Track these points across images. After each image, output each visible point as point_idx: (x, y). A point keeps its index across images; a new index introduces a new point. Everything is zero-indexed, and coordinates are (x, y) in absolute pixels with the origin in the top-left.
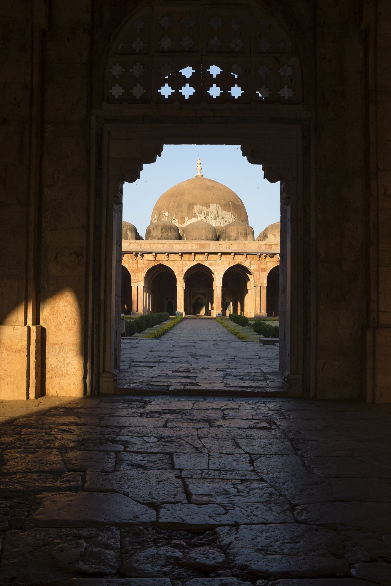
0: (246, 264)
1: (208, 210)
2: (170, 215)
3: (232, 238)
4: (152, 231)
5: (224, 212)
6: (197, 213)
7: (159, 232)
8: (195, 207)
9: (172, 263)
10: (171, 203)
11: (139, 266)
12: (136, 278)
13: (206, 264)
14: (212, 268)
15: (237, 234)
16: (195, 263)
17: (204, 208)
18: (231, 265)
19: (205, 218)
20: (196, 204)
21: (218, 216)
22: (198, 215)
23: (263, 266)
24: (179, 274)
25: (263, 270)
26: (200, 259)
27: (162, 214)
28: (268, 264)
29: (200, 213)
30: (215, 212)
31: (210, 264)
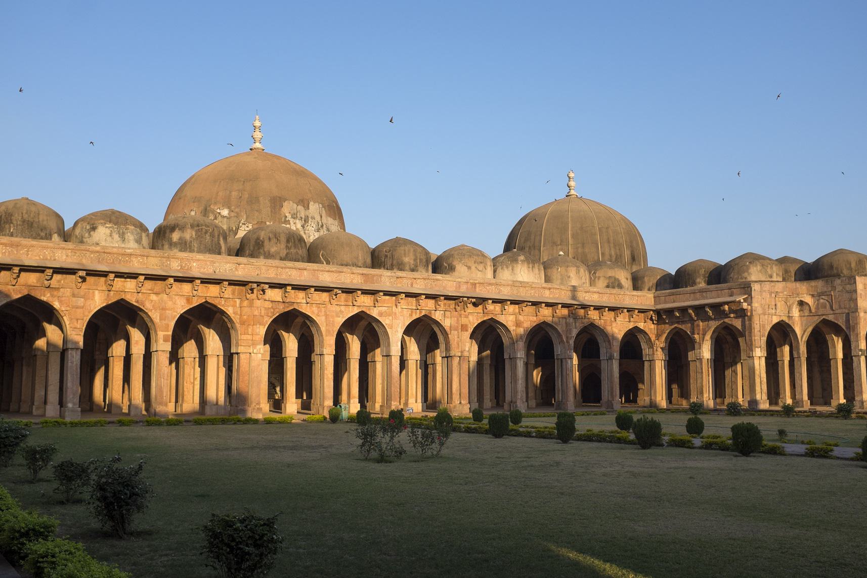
0: (438, 316)
1: (307, 213)
2: (233, 214)
3: (407, 268)
4: (266, 243)
5: (329, 219)
6: (289, 217)
7: (283, 246)
8: (285, 204)
9: (315, 309)
10: (234, 194)
11: (256, 313)
12: (249, 337)
13: (374, 313)
14: (385, 321)
15: (415, 260)
16: (355, 311)
17: (300, 208)
18: (415, 317)
19: (303, 226)
20: (285, 200)
21: (322, 226)
22: (292, 221)
23: (464, 321)
24: (328, 331)
25: (464, 328)
26: (364, 303)
27: (213, 212)
28: (471, 318)
29: (294, 216)
30: (318, 218)
31: (381, 314)
